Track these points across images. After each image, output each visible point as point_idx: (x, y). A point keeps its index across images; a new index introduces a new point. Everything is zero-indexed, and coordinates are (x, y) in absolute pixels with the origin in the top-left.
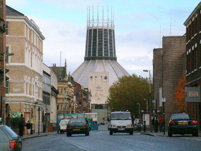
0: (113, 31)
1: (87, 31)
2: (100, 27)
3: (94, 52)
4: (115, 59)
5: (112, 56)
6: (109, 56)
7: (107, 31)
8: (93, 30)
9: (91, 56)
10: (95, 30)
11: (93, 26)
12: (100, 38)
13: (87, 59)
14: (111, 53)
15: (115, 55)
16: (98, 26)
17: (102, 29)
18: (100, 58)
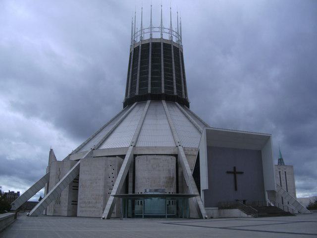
0: (182, 54)
1: (131, 53)
2: (156, 39)
3: (143, 85)
4: (185, 103)
5: (182, 95)
6: (175, 93)
7: (171, 47)
8: (140, 46)
9: (137, 93)
10: (145, 47)
11: (141, 40)
12: (156, 60)
13: (128, 103)
14: (179, 88)
15: (186, 94)
16: (151, 38)
17: (160, 44)
18: (156, 98)
